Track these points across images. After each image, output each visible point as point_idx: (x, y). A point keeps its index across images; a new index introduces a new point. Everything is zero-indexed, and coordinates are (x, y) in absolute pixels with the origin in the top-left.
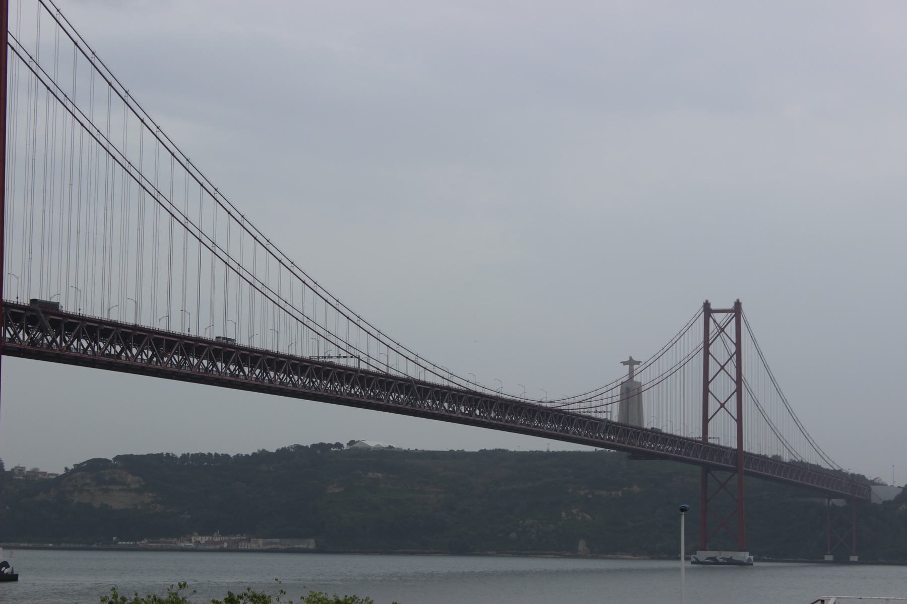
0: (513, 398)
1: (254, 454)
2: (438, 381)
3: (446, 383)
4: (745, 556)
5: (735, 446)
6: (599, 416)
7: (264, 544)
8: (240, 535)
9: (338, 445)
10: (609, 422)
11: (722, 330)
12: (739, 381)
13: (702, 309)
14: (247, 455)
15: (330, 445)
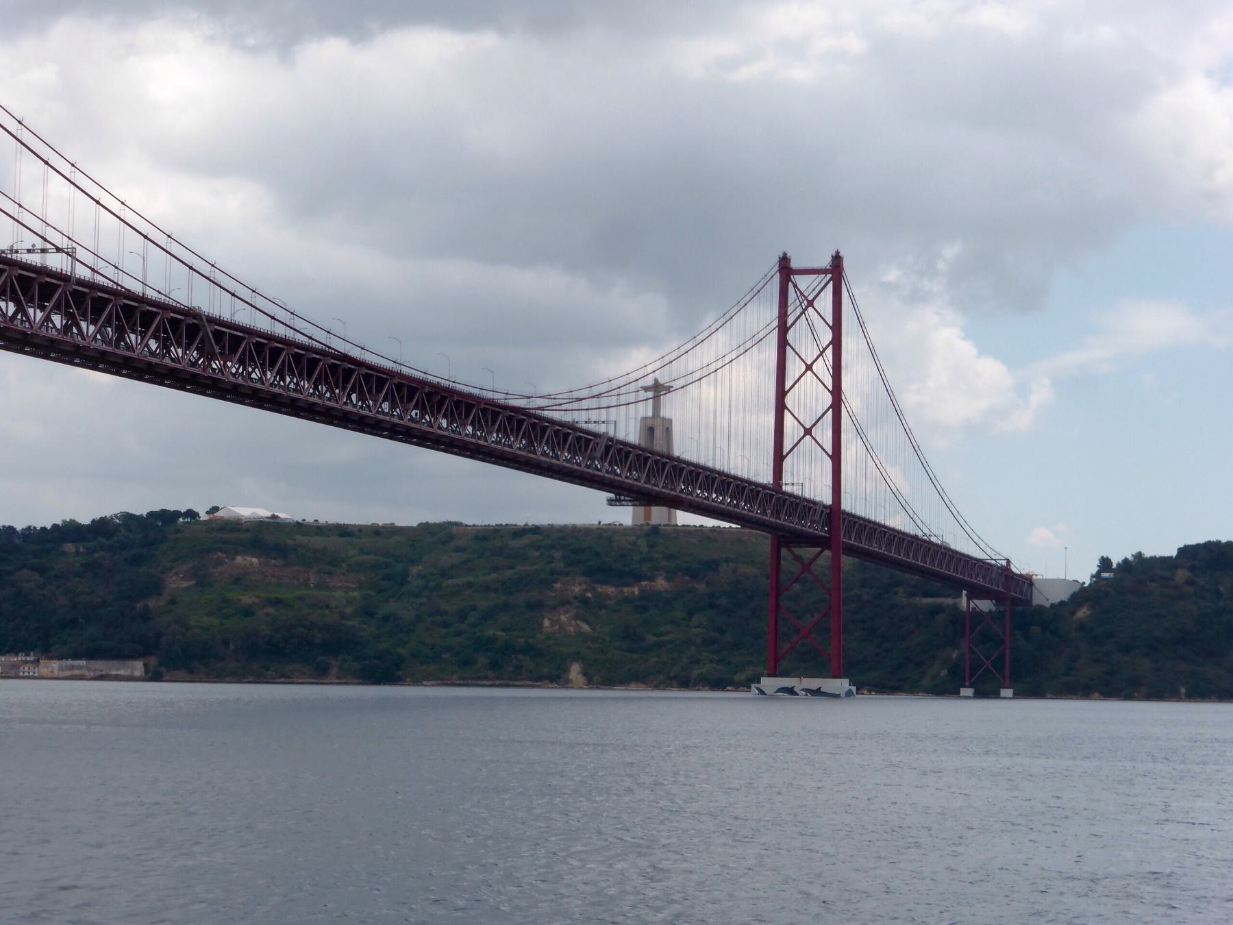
0: (425, 376)
1: (55, 526)
2: (262, 324)
3: (280, 331)
4: (842, 685)
5: (828, 500)
6: (592, 427)
7: (61, 669)
8: (24, 654)
9: (191, 514)
10: (611, 439)
11: (811, 304)
12: (837, 392)
13: (777, 268)
14: (44, 529)
15: (177, 514)
